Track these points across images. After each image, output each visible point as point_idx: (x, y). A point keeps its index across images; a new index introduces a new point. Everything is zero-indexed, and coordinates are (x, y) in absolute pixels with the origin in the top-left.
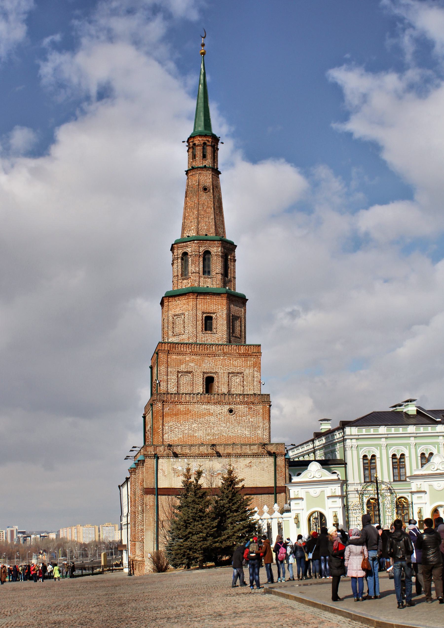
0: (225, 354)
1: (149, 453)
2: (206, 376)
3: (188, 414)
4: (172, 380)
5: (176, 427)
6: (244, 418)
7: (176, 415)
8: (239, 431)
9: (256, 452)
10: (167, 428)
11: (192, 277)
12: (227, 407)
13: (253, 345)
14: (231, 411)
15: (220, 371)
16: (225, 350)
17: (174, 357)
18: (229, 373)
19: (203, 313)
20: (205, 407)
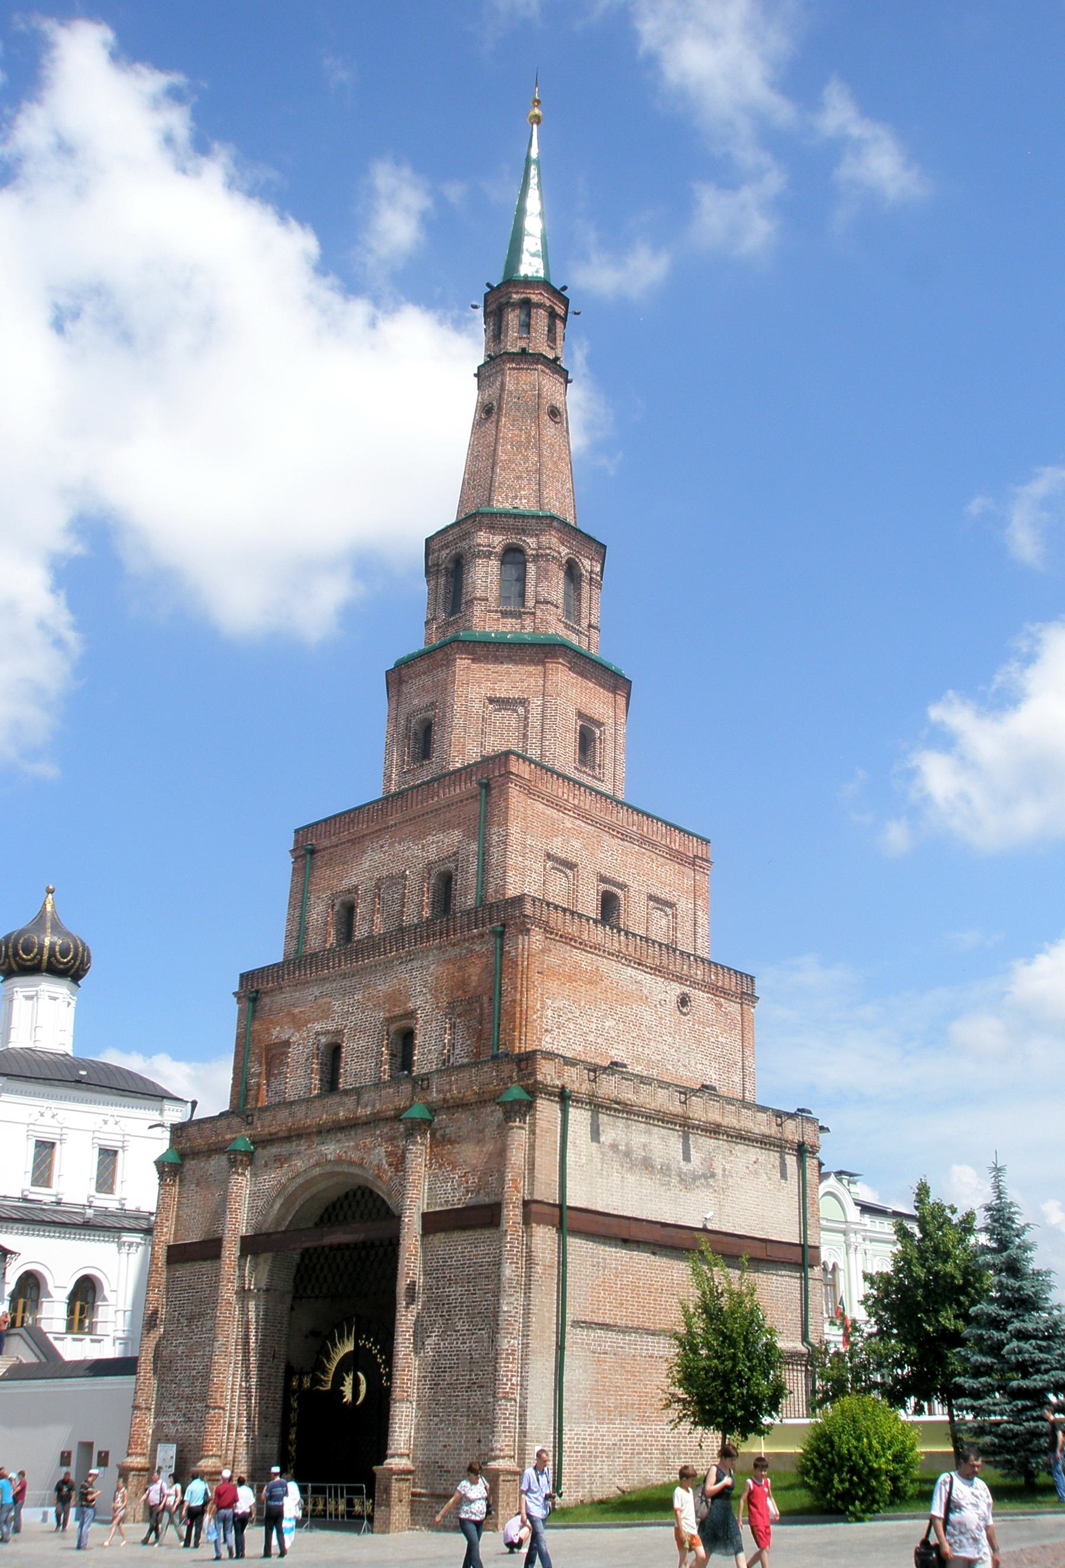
0: (644, 841)
1: (549, 1078)
2: (603, 887)
3: (596, 983)
4: (534, 875)
5: (570, 1016)
6: (708, 1030)
7: (571, 980)
8: (699, 1066)
9: (767, 1132)
10: (549, 1013)
11: (539, 613)
12: (676, 989)
13: (697, 837)
14: (684, 1001)
15: (634, 885)
16: (645, 829)
17: (541, 806)
18: (651, 898)
19: (580, 715)
20: (634, 972)
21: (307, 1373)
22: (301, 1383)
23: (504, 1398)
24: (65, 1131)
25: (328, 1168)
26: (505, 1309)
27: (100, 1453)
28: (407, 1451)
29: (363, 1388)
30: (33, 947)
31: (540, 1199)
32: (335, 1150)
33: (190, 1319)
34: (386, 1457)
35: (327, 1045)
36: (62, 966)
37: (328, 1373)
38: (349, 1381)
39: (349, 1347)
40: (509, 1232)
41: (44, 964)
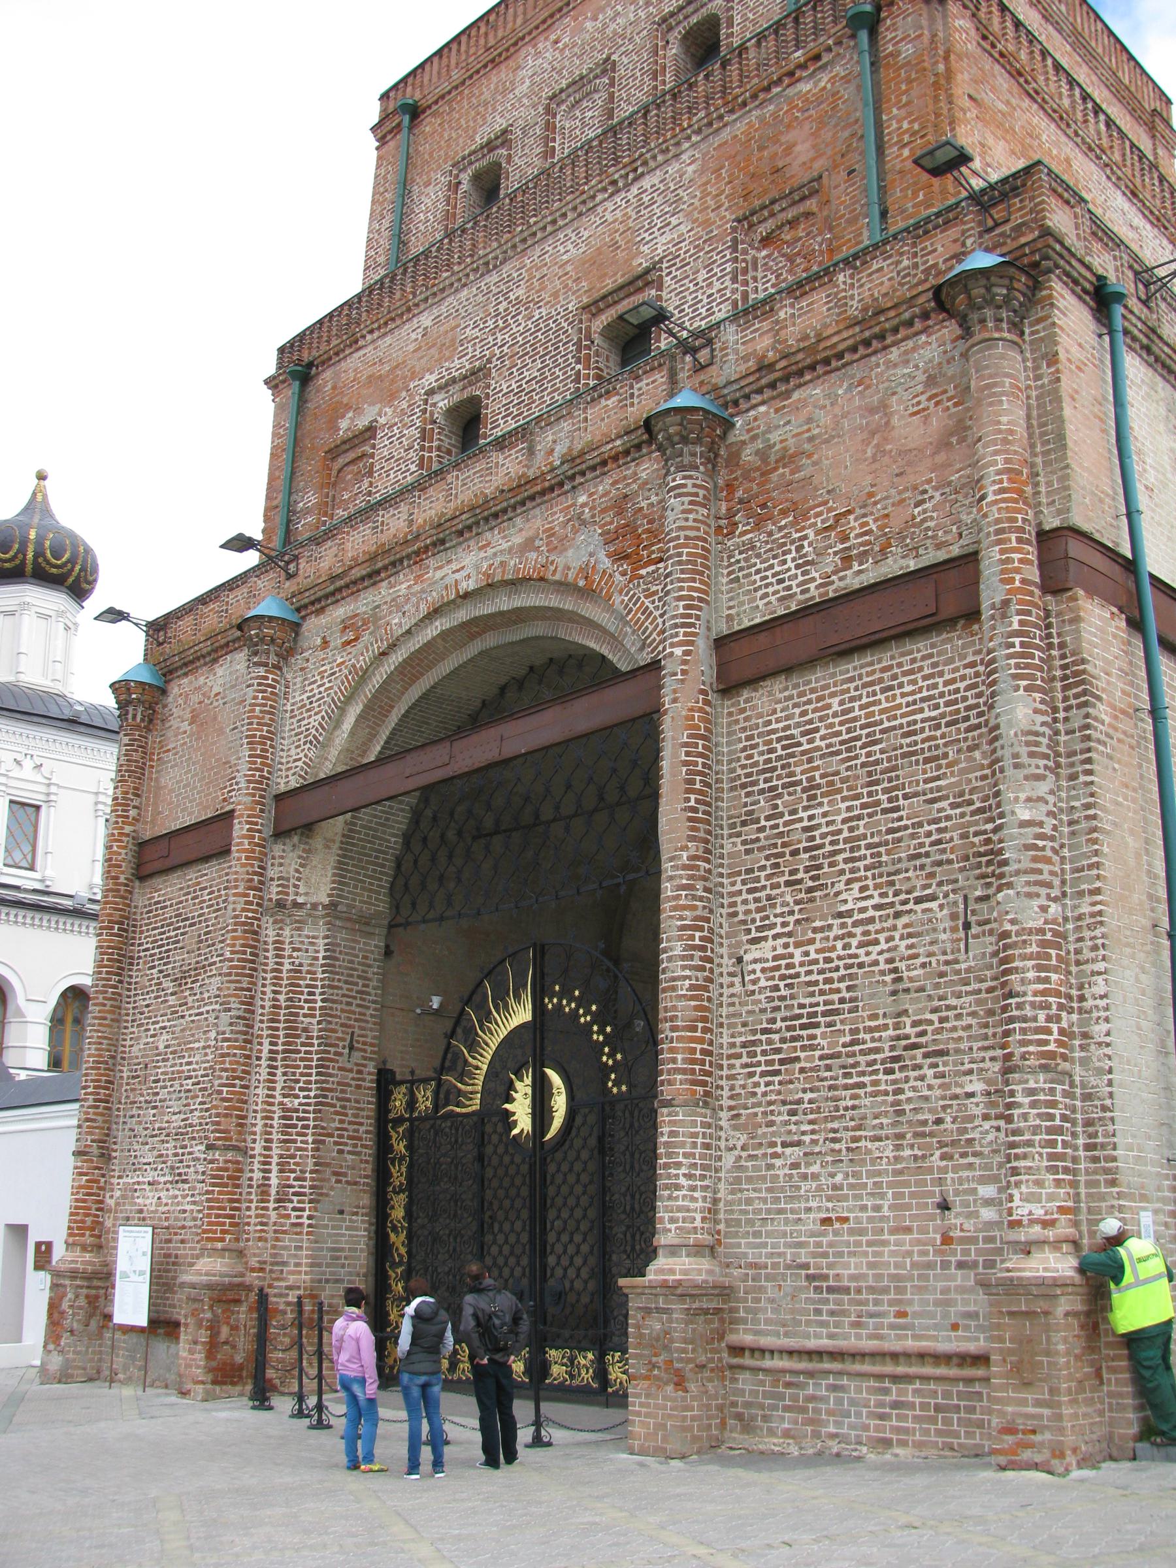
21: (426, 1081)
22: (412, 1104)
23: (1045, 1068)
24: (53, 789)
25: (462, 615)
26: (1025, 815)
27: (38, 1245)
28: (707, 1239)
29: (560, 1103)
30: (13, 542)
31: (1085, 527)
32: (477, 567)
33: (179, 981)
34: (651, 1253)
35: (451, 412)
36: (54, 571)
37: (472, 1076)
38: (523, 1090)
39: (522, 1014)
40: (1014, 607)
41: (29, 568)
